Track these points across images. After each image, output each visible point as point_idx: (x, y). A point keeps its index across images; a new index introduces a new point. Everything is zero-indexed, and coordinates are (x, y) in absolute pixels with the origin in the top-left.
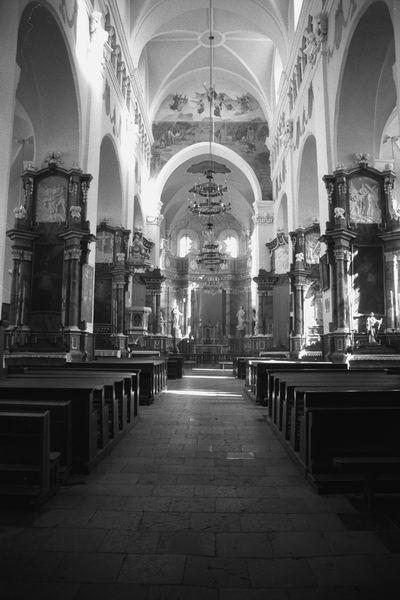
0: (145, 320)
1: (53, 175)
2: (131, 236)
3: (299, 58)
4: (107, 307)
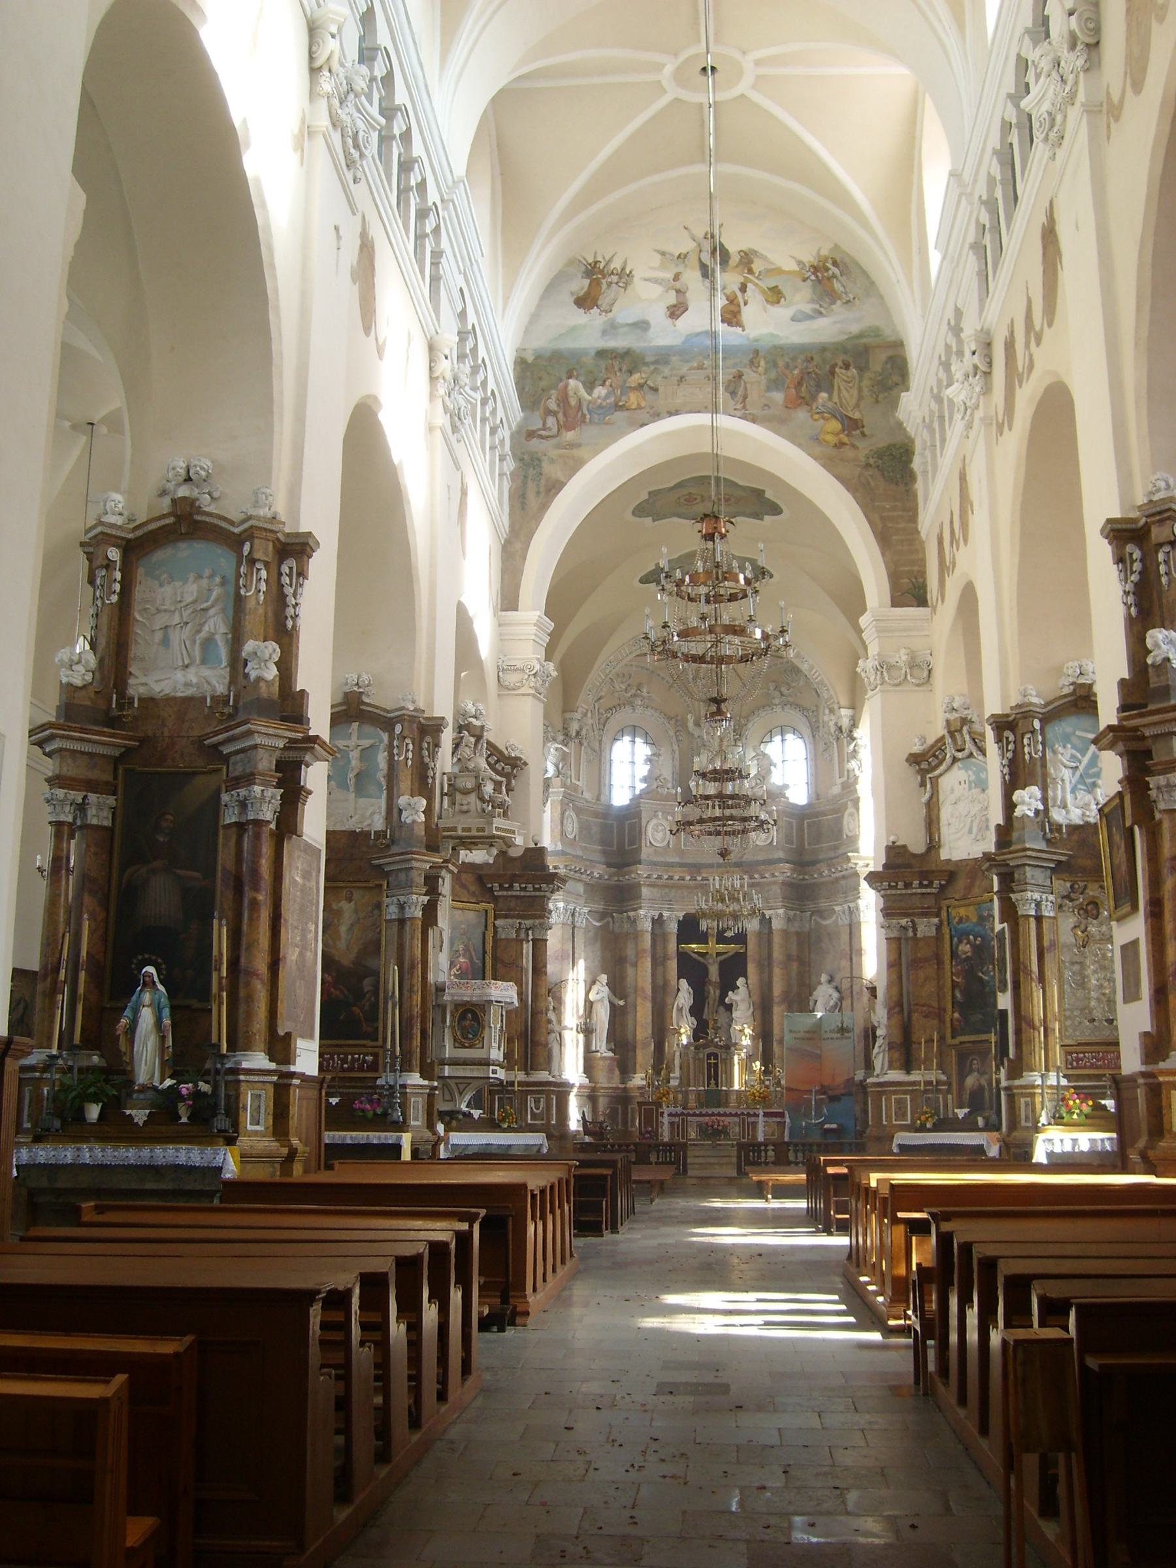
0: (495, 1025)
1: (183, 537)
2: (447, 737)
3: (1006, 127)
4: (367, 983)
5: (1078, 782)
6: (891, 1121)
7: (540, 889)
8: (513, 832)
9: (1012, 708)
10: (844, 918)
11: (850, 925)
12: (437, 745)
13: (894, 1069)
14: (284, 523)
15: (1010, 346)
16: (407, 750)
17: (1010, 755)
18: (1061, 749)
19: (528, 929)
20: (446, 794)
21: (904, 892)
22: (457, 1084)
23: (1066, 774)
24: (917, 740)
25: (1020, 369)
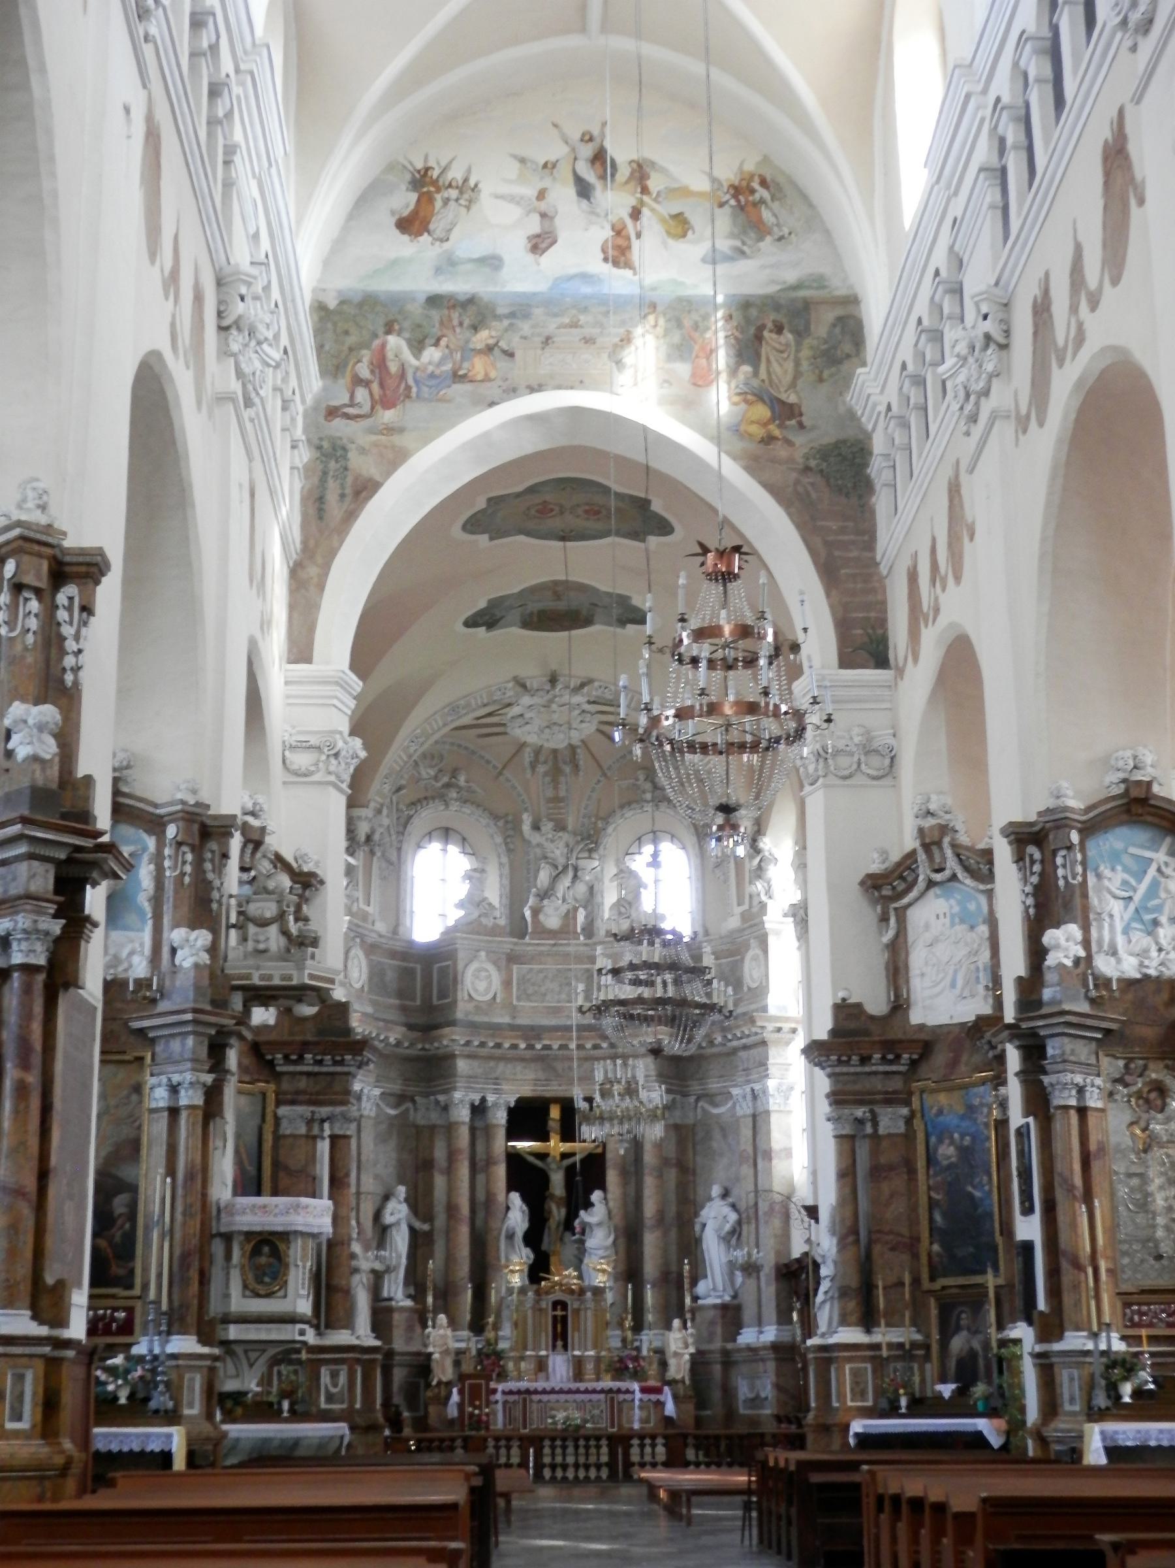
2: (236, 843)
5: (1132, 919)
6: (845, 1402)
7: (341, 1063)
8: (332, 981)
9: (1040, 814)
10: (744, 1105)
11: (754, 1116)
12: (225, 856)
13: (849, 1325)
14: (65, 534)
15: (1042, 310)
16: (184, 863)
17: (1035, 879)
18: (1107, 873)
19: (323, 1121)
20: (234, 926)
21: (859, 1069)
22: (246, 1352)
23: (1116, 907)
24: (876, 855)
25: (1060, 341)
